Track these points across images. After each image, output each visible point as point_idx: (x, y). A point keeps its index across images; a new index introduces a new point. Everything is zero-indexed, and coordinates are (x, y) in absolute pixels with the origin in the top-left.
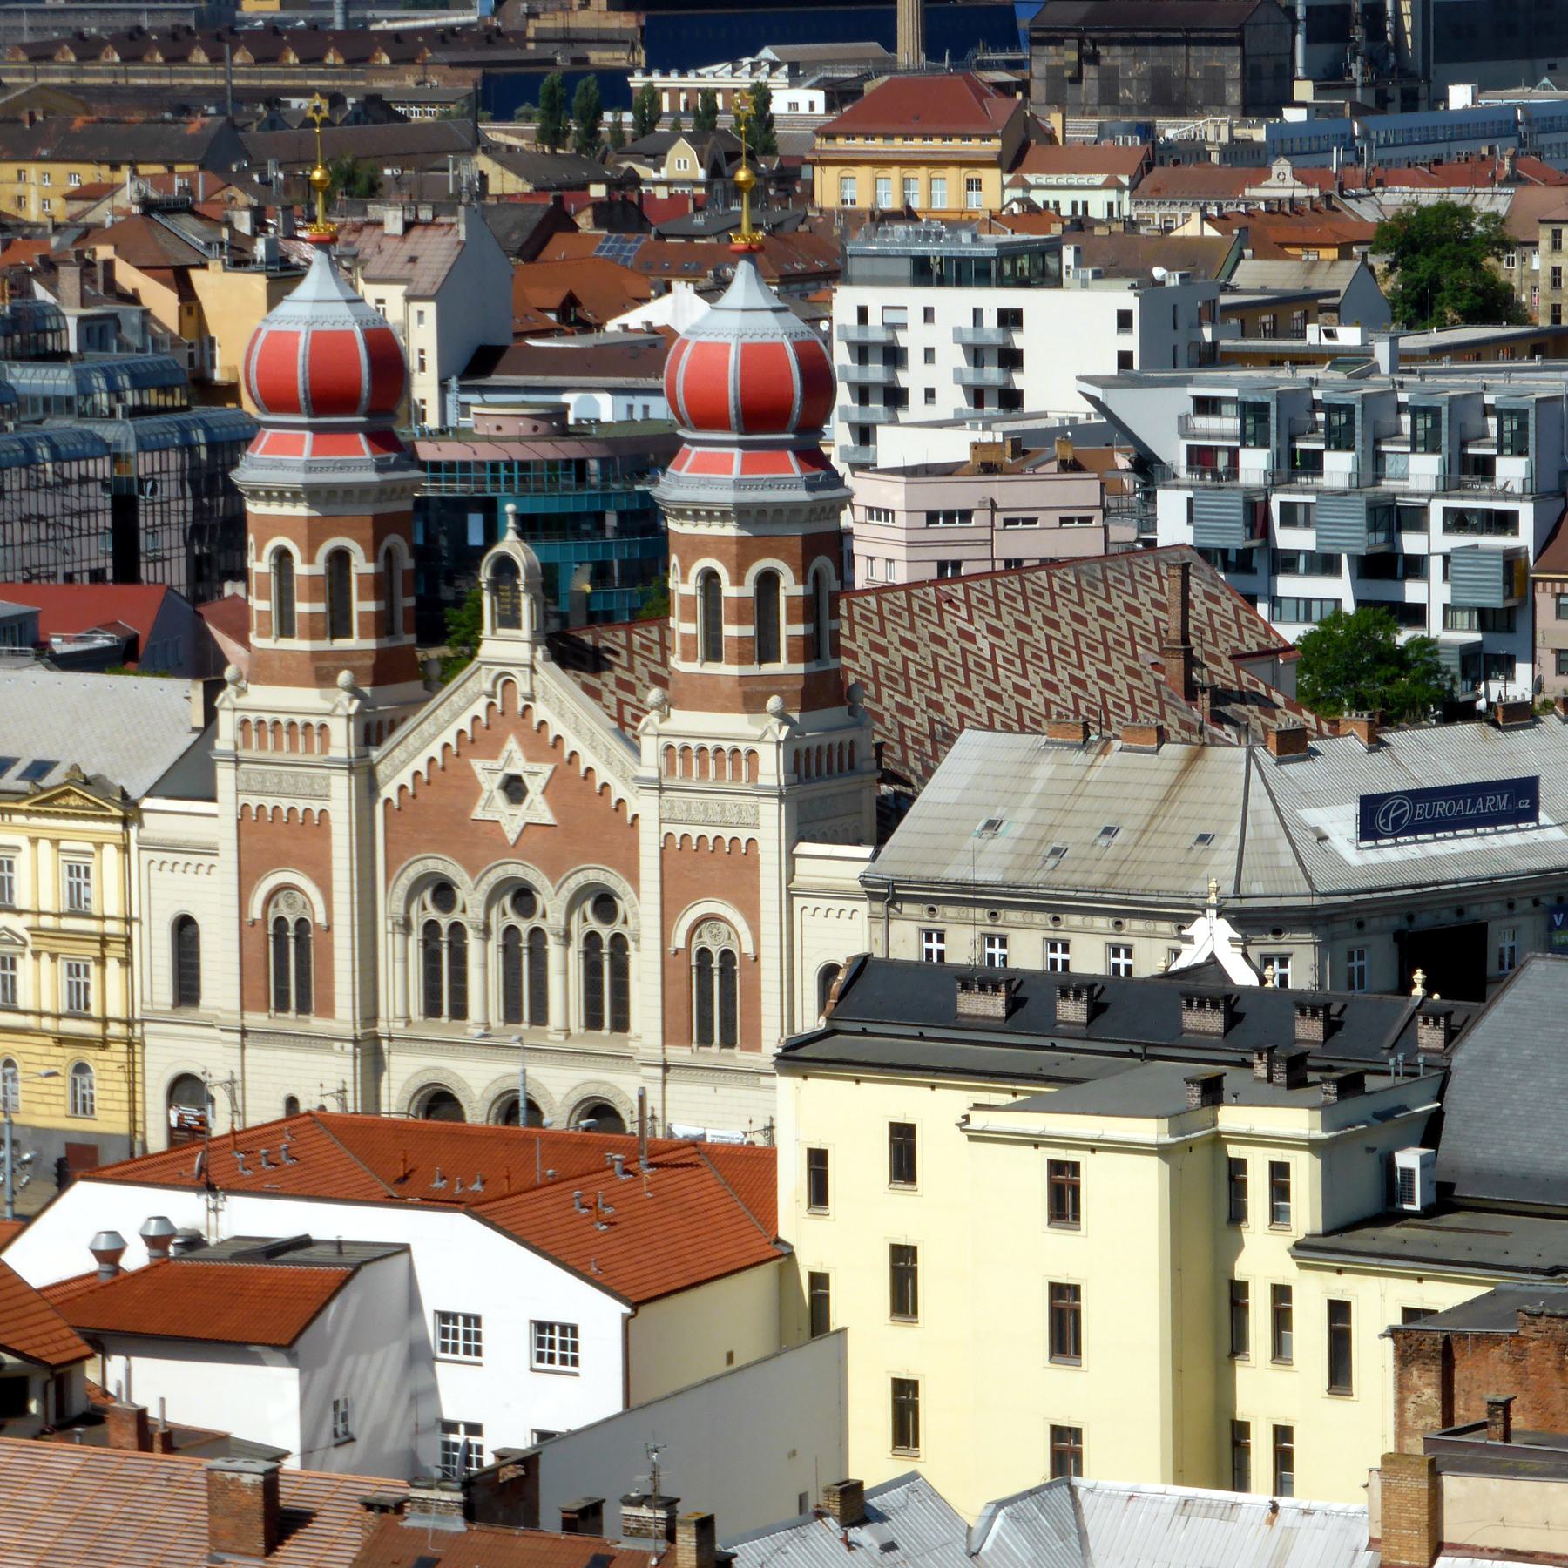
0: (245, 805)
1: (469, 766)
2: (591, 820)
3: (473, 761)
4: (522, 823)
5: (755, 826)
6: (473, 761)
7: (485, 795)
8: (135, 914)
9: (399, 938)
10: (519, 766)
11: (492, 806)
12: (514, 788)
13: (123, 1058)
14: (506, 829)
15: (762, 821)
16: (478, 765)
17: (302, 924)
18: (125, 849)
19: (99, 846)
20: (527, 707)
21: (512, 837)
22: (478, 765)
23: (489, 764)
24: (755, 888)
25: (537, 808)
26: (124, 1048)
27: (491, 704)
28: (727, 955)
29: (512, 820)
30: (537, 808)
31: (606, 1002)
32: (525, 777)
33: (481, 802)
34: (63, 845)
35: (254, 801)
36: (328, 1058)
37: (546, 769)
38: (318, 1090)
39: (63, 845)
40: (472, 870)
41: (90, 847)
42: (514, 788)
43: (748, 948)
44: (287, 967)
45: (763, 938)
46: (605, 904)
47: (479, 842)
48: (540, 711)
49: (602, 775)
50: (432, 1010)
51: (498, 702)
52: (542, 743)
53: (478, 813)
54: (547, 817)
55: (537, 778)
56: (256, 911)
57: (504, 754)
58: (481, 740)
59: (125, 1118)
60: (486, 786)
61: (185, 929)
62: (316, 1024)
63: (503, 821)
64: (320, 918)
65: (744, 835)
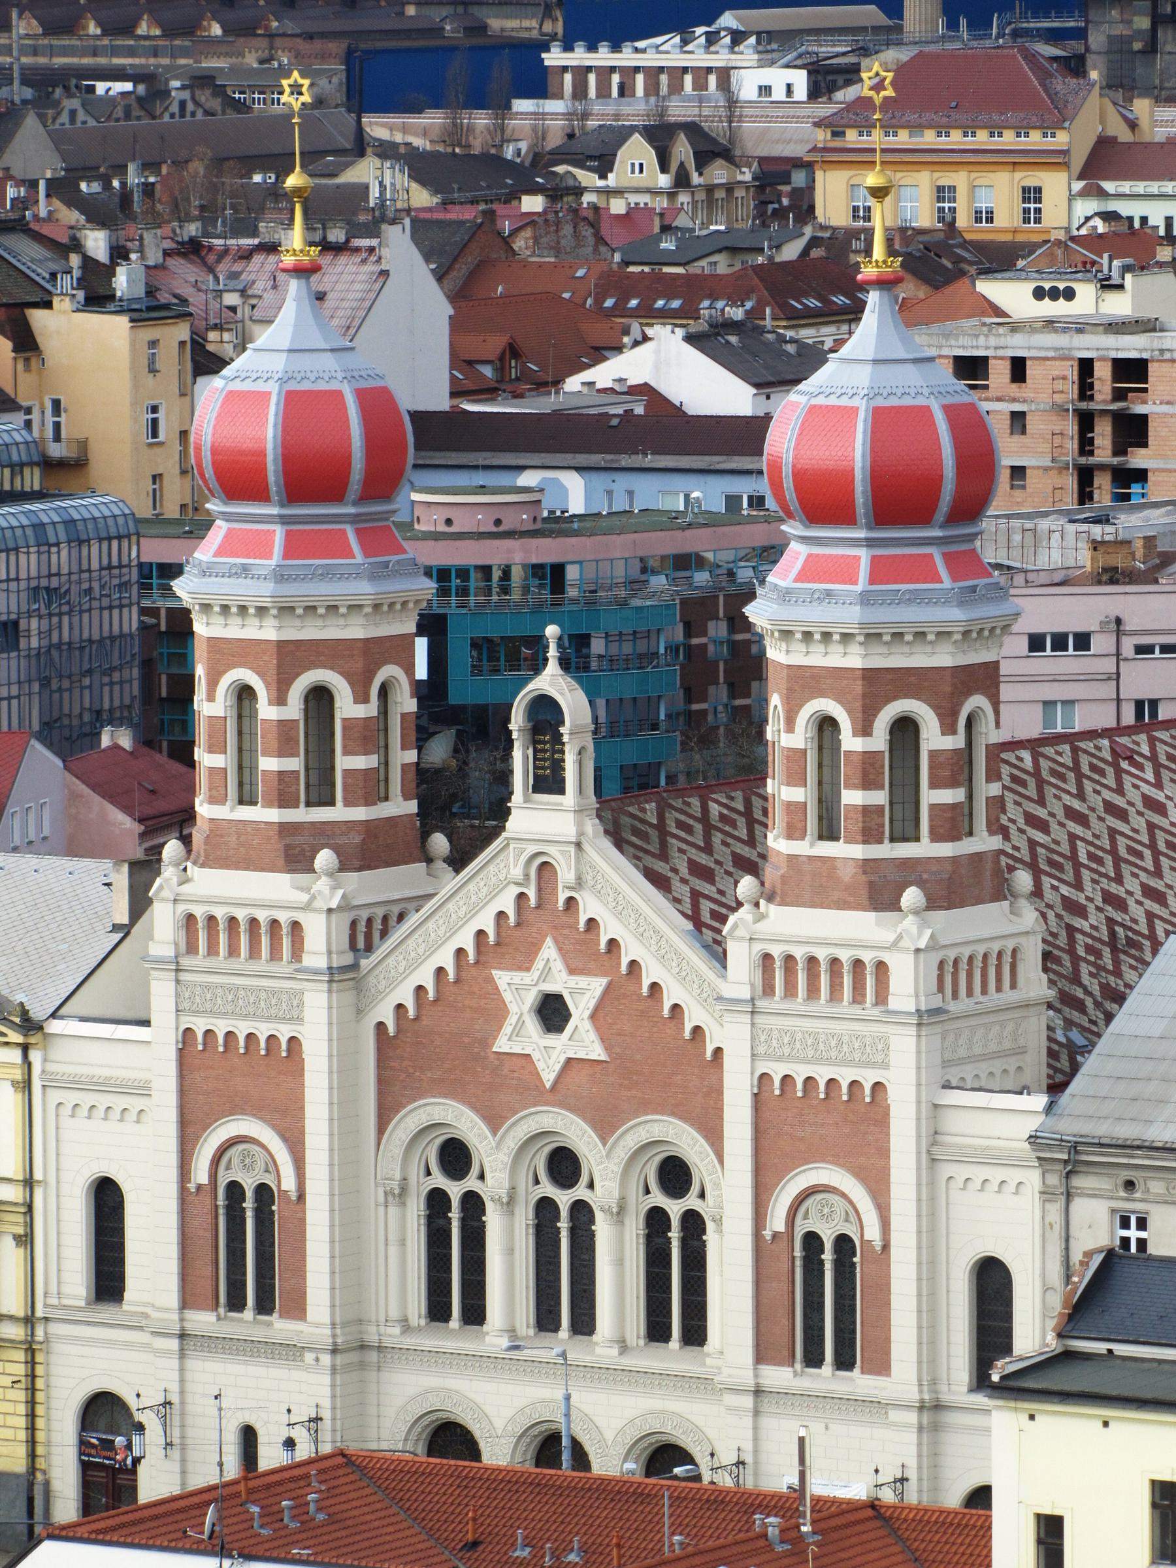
0: (188, 1030)
1: (490, 980)
2: (658, 1060)
3: (496, 973)
4: (562, 1059)
5: (885, 1065)
6: (496, 973)
7: (512, 1020)
8: (38, 1175)
9: (393, 1211)
10: (560, 982)
11: (518, 1034)
12: (552, 1011)
13: (20, 1370)
14: (540, 1066)
16: (503, 978)
17: (263, 1191)
18: (26, 1085)
20: (570, 901)
21: (548, 1078)
22: (503, 978)
23: (517, 977)
24: (884, 1152)
25: (582, 1039)
26: (20, 1356)
27: (522, 896)
29: (549, 1053)
30: (582, 1039)
31: (675, 1306)
33: (507, 1029)
35: (200, 1026)
36: (297, 1375)
37: (595, 986)
38: (285, 1418)
40: (494, 1121)
42: (552, 1011)
43: (873, 1233)
44: (244, 1252)
46: (675, 1175)
47: (501, 1087)
48: (589, 907)
49: (672, 994)
50: (438, 1311)
51: (532, 893)
52: (590, 949)
53: (502, 1044)
54: (596, 1051)
55: (583, 994)
56: (201, 1175)
57: (539, 964)
59: (22, 1451)
60: (513, 1008)
61: (107, 1199)
62: (280, 1327)
63: (536, 1056)
64: (289, 1183)
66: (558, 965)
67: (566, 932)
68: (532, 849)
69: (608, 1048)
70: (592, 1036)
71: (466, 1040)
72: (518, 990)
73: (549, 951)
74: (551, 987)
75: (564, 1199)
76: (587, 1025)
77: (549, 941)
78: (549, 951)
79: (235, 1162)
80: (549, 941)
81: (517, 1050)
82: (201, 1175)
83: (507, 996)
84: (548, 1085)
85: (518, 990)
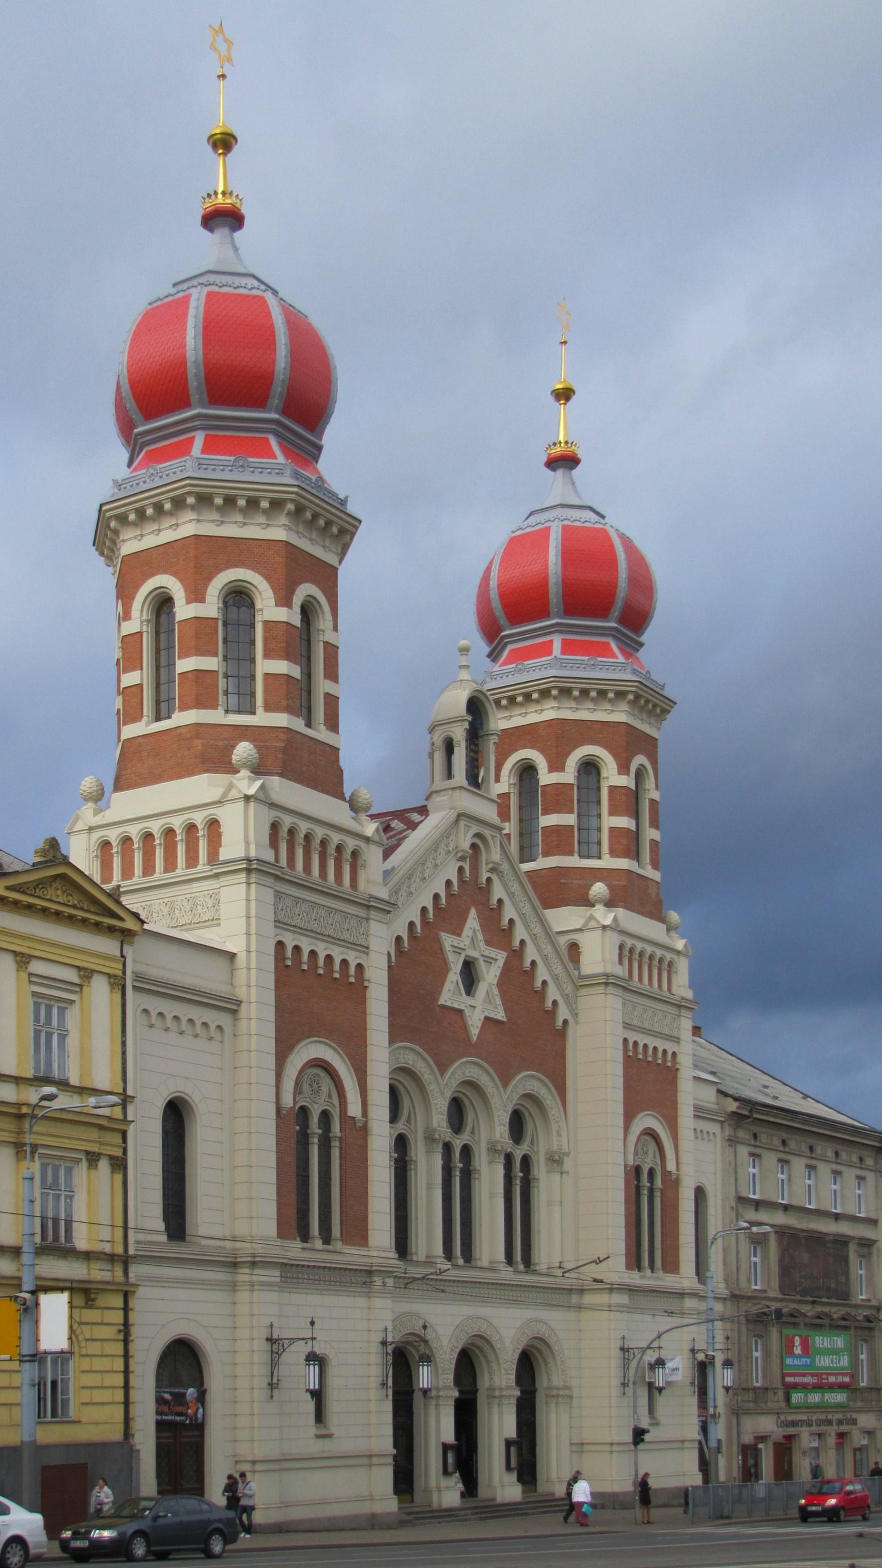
4: (482, 1018)
8: (130, 1092)
11: (451, 993)
16: (448, 940)
19: (87, 974)
20: (489, 880)
22: (448, 940)
32: (482, 965)
34: (36, 967)
37: (501, 957)
39: (36, 967)
41: (72, 976)
42: (469, 975)
54: (501, 1015)
57: (467, 932)
65: (670, 1047)
66: (480, 936)
68: (475, 828)
73: (472, 922)
74: (473, 953)
78: (472, 922)
81: (456, 1005)
82: (288, 1100)
83: (451, 957)
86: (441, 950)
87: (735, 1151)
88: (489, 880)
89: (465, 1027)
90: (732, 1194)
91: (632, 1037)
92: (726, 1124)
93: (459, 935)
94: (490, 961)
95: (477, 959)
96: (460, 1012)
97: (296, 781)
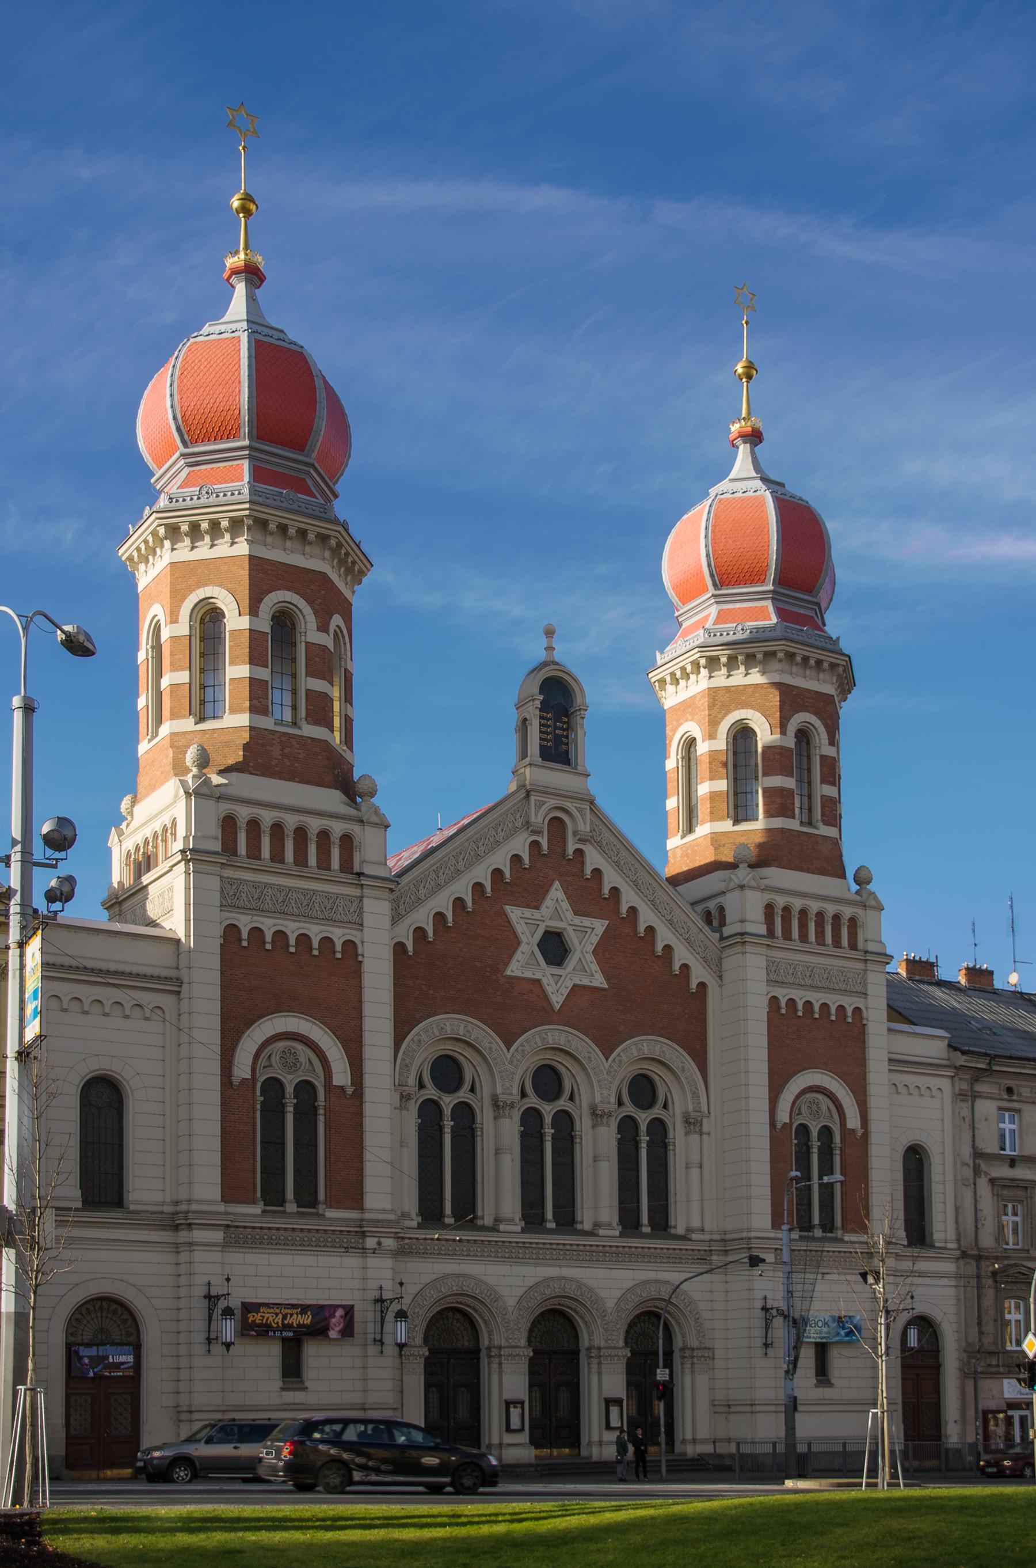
11: (524, 963)
14: (549, 990)
15: (871, 989)
16: (515, 914)
17: (305, 1088)
20: (579, 852)
21: (557, 1000)
22: (515, 914)
23: (528, 913)
25: (584, 969)
27: (535, 845)
28: (826, 1132)
30: (584, 969)
32: (572, 937)
37: (599, 926)
42: (554, 948)
45: (873, 1114)
48: (593, 859)
52: (590, 895)
53: (515, 968)
54: (599, 981)
57: (548, 902)
58: (523, 884)
63: (545, 981)
64: (342, 1076)
65: (850, 1003)
66: (565, 905)
67: (570, 879)
68: (552, 802)
69: (608, 979)
70: (595, 967)
71: (479, 965)
72: (526, 923)
73: (556, 892)
74: (556, 925)
75: (548, 1110)
76: (590, 957)
77: (557, 884)
78: (556, 892)
79: (275, 1060)
80: (557, 884)
83: (520, 928)
84: (557, 1007)
85: (526, 923)
86: (509, 923)
87: (973, 1107)
88: (579, 852)
89: (546, 997)
90: (966, 1151)
91: (783, 994)
92: (956, 1078)
93: (537, 908)
94: (583, 931)
95: (565, 929)
96: (539, 981)
97: (263, 775)
